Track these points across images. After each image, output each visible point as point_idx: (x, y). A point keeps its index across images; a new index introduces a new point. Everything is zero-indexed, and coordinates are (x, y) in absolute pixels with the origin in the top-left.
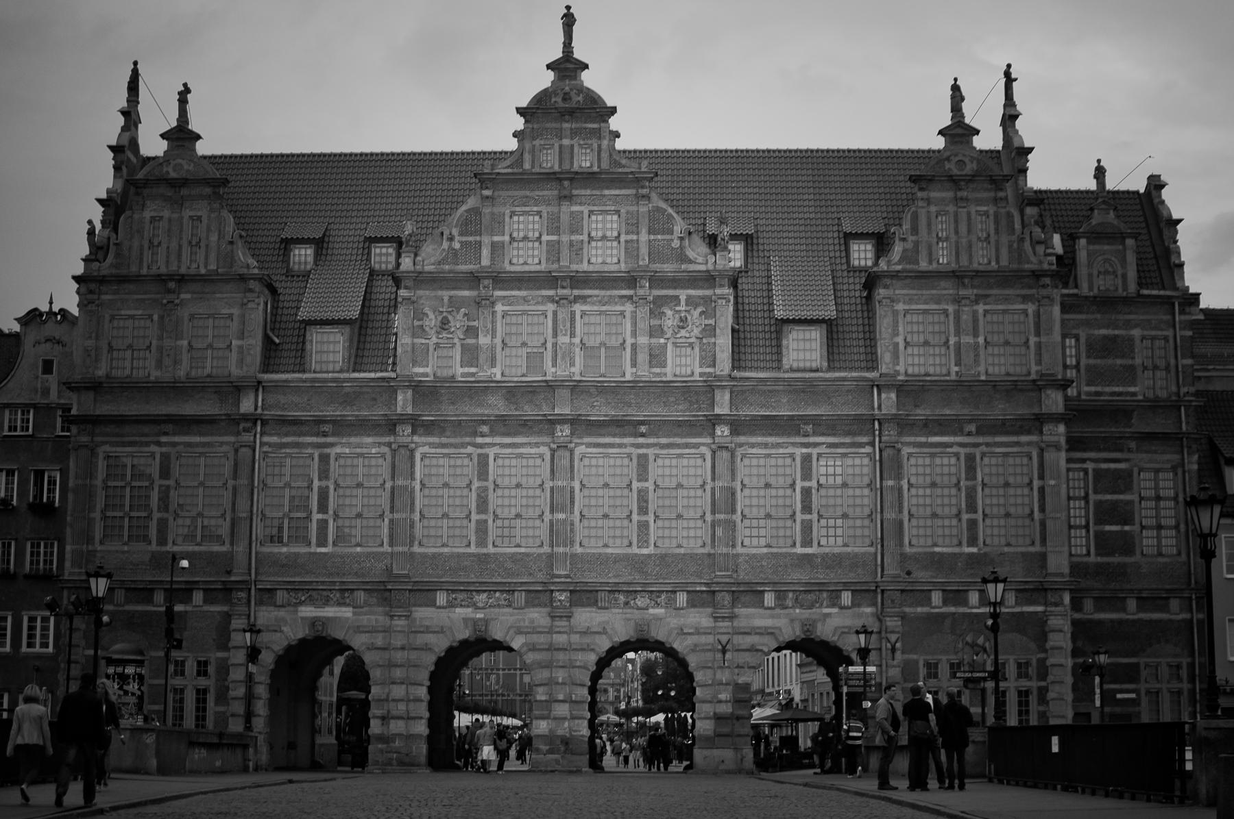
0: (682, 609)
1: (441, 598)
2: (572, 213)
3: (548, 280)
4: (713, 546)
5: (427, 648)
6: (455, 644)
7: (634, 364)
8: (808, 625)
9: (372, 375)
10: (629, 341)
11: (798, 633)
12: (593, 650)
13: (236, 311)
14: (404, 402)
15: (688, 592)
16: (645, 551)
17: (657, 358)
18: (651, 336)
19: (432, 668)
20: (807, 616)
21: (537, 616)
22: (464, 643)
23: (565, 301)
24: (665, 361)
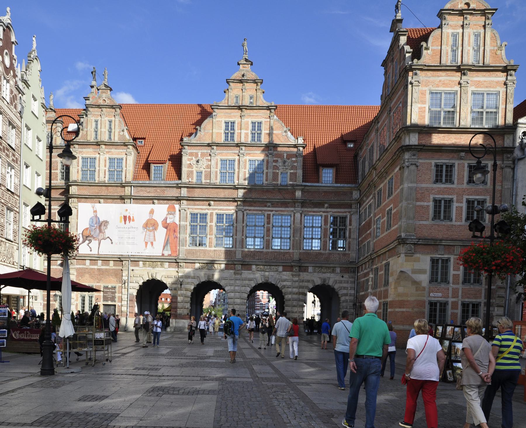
0: (281, 272)
4: (293, 249)
7: (266, 180)
8: (324, 280)
9: (173, 182)
10: (265, 171)
13: (124, 156)
14: (184, 192)
16: (268, 250)
19: (192, 291)
20: (323, 276)
22: (203, 283)
23: (242, 155)
24: (278, 179)
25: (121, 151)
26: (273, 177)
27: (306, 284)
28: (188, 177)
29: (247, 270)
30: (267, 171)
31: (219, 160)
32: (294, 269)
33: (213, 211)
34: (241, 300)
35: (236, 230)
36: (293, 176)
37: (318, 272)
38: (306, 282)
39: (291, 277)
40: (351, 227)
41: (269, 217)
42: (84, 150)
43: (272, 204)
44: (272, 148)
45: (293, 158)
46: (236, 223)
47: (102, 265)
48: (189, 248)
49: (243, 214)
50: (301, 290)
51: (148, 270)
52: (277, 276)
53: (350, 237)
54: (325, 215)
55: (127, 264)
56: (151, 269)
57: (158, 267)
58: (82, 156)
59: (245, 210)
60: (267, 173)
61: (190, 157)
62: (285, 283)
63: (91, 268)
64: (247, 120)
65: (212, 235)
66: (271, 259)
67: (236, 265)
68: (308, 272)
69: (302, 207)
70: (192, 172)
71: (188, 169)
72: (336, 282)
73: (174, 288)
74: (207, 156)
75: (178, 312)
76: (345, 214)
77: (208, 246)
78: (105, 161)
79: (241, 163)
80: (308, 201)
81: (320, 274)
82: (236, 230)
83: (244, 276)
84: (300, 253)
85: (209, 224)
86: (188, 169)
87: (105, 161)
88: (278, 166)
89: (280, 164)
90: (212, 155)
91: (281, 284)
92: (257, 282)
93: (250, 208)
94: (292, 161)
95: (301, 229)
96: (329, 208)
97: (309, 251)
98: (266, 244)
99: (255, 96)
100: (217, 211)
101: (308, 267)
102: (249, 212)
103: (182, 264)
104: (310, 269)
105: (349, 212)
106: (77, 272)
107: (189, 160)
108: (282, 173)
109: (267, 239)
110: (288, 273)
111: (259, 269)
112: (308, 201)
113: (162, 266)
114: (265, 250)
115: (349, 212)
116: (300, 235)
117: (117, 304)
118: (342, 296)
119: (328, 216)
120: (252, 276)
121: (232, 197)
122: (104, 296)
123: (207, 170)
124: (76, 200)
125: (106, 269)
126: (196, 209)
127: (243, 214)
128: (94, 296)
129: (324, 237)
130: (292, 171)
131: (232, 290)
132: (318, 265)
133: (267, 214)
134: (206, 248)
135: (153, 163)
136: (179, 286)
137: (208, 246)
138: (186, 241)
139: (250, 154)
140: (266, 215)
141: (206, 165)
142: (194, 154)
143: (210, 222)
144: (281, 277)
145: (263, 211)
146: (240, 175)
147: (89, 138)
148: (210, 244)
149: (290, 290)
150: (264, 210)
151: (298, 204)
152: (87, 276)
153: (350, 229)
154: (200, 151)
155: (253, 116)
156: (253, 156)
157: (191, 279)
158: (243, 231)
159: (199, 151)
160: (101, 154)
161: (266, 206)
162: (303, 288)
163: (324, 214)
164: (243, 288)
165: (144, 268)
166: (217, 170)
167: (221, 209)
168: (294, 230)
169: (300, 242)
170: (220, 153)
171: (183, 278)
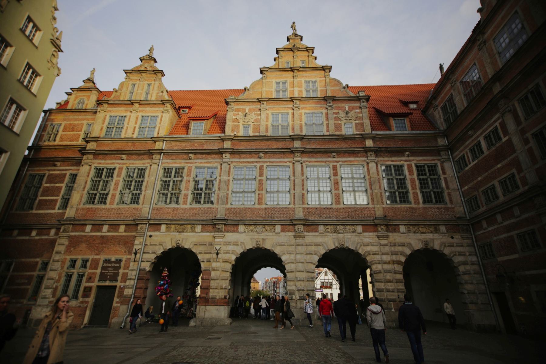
0: (361, 233)
1: (241, 228)
3: (292, 99)
4: (373, 204)
5: (233, 252)
6: (245, 251)
8: (426, 243)
11: (421, 246)
12: (315, 254)
14: (227, 145)
15: (362, 225)
16: (339, 206)
17: (338, 127)
18: (335, 121)
19: (234, 263)
21: (287, 237)
23: (297, 109)
25: (158, 109)
26: (335, 127)
27: (400, 249)
29: (312, 232)
30: (327, 122)
31: (270, 114)
32: (380, 229)
33: (263, 164)
35: (294, 184)
36: (360, 126)
37: (414, 232)
38: (399, 246)
39: (377, 239)
40: (445, 176)
41: (335, 168)
42: (114, 109)
44: (331, 101)
46: (294, 176)
47: (108, 231)
48: (231, 206)
49: (302, 166)
50: (394, 258)
51: (172, 235)
52: (357, 239)
53: (448, 188)
54: (408, 165)
55: (144, 227)
56: (177, 234)
57: (186, 232)
58: (110, 114)
59: (304, 162)
60: (328, 125)
63: (91, 236)
64: (300, 80)
65: (262, 190)
66: (345, 217)
67: (297, 226)
68: (399, 232)
69: (376, 156)
70: (238, 126)
71: (233, 124)
72: (443, 244)
73: (207, 259)
74: (256, 111)
75: (211, 294)
76: (433, 162)
77: (256, 204)
78: (137, 118)
79: (296, 116)
80: (383, 149)
81: (418, 234)
82: (294, 184)
84: (384, 209)
86: (233, 124)
87: (137, 118)
90: (262, 110)
91: (363, 250)
92: (327, 247)
93: (310, 159)
94: (356, 112)
95: (379, 180)
96: (411, 156)
97: (396, 206)
99: (308, 61)
101: (399, 225)
103: (220, 227)
104: (402, 229)
105: (439, 160)
106: (70, 242)
107: (234, 115)
108: (345, 123)
109: (335, 193)
110: (371, 234)
111: (329, 230)
112: (383, 149)
113: (193, 230)
114: (334, 206)
116: (380, 187)
117: (119, 284)
118: (459, 266)
119: (411, 165)
121: (289, 148)
122: (101, 273)
123: (256, 123)
124: (91, 156)
125: (114, 236)
126: (241, 162)
127: (302, 166)
128: (86, 274)
130: (357, 122)
131: (292, 259)
133: (333, 165)
134: (254, 207)
135: (193, 120)
136: (215, 255)
138: (227, 198)
139: (305, 108)
140: (331, 167)
141: (254, 119)
143: (260, 176)
144: (362, 239)
145: (327, 163)
146: (296, 127)
147: (121, 99)
148: (260, 201)
149: (378, 257)
150: (328, 161)
151: (371, 153)
152: (84, 245)
154: (248, 107)
155: (306, 76)
157: (232, 246)
159: (247, 108)
160: (133, 112)
161: (330, 157)
162: (398, 254)
163: (406, 163)
164: (309, 256)
165: (166, 233)
166: (267, 123)
167: (273, 162)
168: (370, 182)
169: (381, 196)
170: (271, 108)
171: (220, 245)
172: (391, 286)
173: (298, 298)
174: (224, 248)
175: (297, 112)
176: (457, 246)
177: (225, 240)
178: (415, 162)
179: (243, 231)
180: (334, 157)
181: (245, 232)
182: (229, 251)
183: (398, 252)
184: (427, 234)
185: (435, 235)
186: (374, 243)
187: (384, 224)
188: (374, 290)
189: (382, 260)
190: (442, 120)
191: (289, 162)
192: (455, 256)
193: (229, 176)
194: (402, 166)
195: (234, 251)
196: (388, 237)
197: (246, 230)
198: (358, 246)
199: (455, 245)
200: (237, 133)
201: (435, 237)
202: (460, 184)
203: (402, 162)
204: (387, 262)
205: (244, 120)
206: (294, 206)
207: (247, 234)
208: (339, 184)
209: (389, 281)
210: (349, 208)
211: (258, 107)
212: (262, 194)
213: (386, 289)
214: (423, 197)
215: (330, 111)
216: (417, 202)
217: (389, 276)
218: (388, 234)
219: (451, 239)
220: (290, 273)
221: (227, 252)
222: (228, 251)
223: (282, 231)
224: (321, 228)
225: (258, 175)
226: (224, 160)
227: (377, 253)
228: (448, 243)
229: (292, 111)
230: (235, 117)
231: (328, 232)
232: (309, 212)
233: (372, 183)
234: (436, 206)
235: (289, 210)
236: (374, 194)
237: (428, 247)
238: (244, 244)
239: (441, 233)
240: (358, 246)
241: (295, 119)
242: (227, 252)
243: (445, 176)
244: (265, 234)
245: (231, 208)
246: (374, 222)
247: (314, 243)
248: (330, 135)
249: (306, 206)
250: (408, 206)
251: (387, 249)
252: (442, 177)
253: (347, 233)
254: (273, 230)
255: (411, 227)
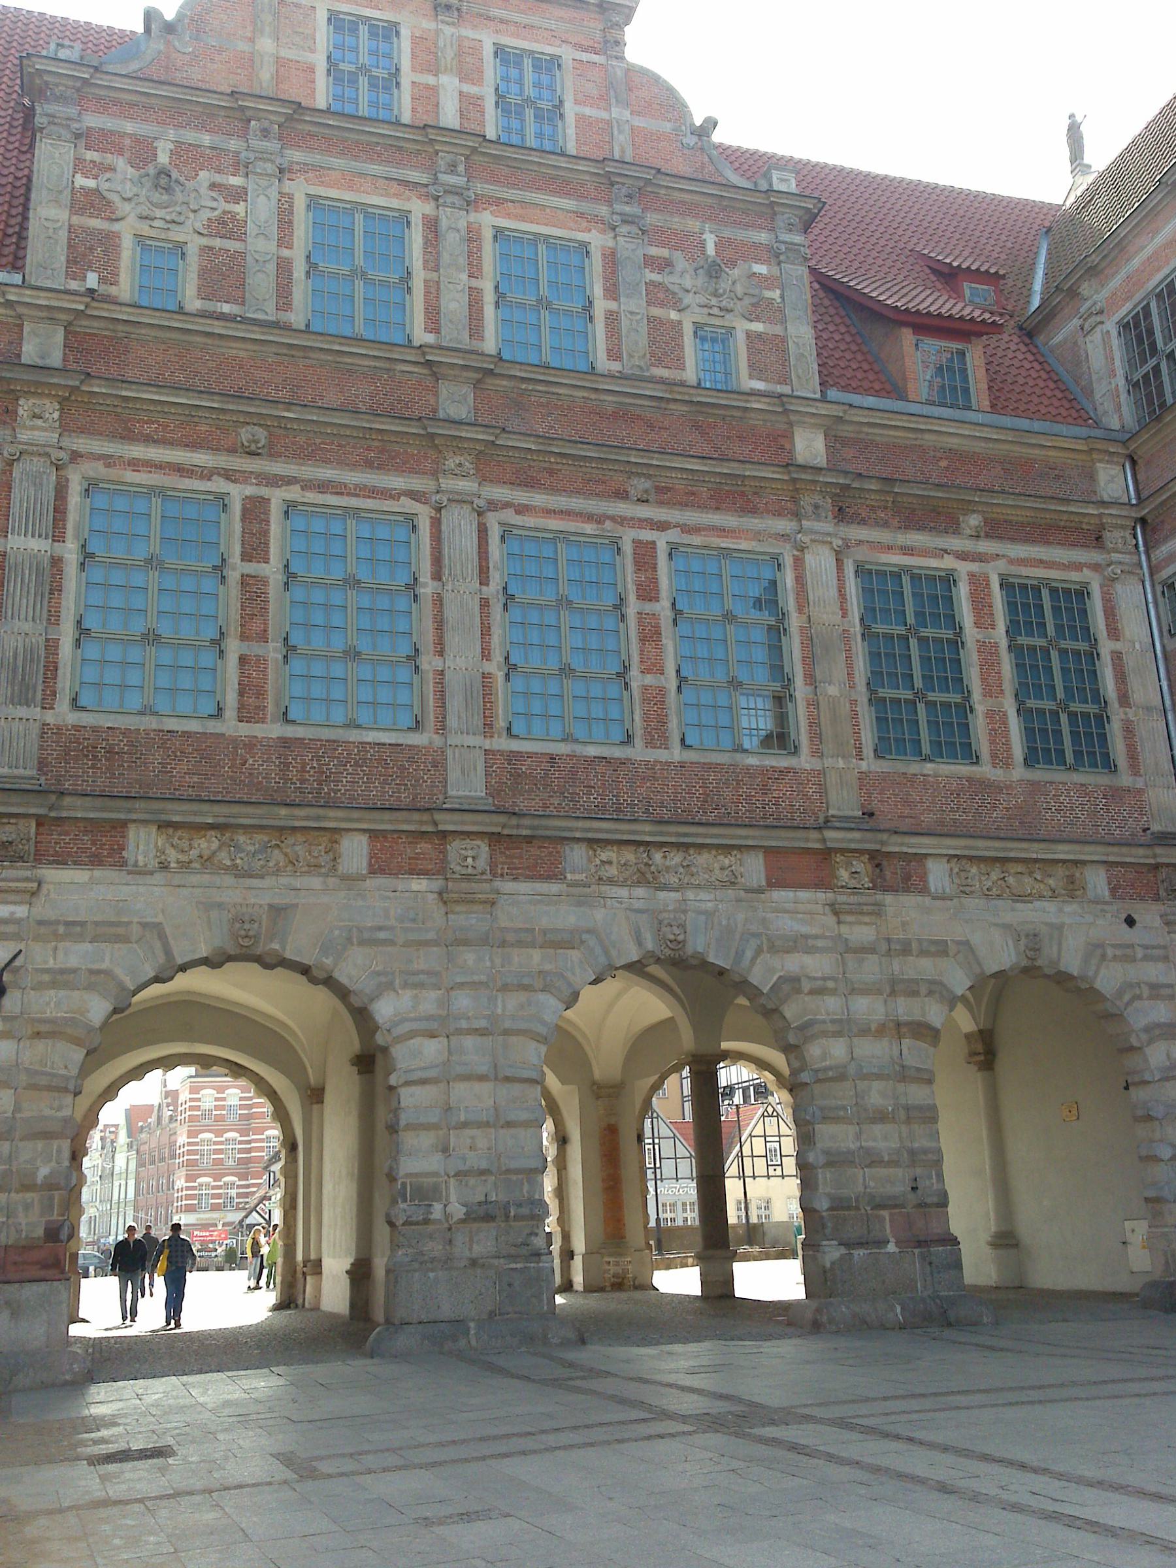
2: (461, 39)
4: (817, 753)
7: (614, 354)
8: (1033, 941)
10: (601, 306)
15: (768, 851)
16: (662, 755)
27: (925, 967)
28: (71, 262)
30: (613, 305)
31: (300, 203)
32: (844, 874)
33: (265, 491)
34: (505, 1092)
38: (923, 953)
39: (831, 920)
40: (1118, 646)
43: (660, 490)
45: (758, 260)
46: (437, 576)
48: (72, 718)
49: (483, 531)
50: (905, 1008)
52: (741, 917)
54: (971, 575)
59: (493, 506)
60: (612, 318)
61: (91, 155)
62: (793, 963)
65: (263, 637)
67: (455, 848)
68: (924, 890)
70: (110, 241)
72: (1096, 950)
76: (1074, 576)
77: (230, 713)
79: (452, 242)
81: (1000, 903)
82: (440, 624)
83: (508, 916)
84: (863, 776)
85: (238, 568)
88: (676, 289)
89: (688, 282)
92: (606, 952)
93: (521, 496)
95: (846, 636)
97: (914, 768)
98: (646, 718)
100: (294, 493)
102: (518, 520)
104: (938, 875)
105: (1096, 567)
107: (79, 165)
108: (698, 327)
109: (645, 688)
110: (804, 895)
111: (613, 871)
115: (1096, 567)
120: (567, 917)
123: (218, 243)
127: (483, 531)
129: (987, 693)
130: (758, 327)
131: (430, 1018)
132: (984, 847)
133: (637, 543)
134: (214, 727)
137: (230, 713)
138: (52, 669)
139: (499, 202)
140: (628, 548)
141: (205, 215)
142: (127, 142)
143: (246, 557)
144: (764, 921)
145: (608, 524)
149: (831, 1005)
150: (613, 518)
153: (1117, 657)
154: (172, 134)
155: (502, 21)
156: (522, 219)
158: (486, 631)
161: (621, 495)
162: (915, 993)
163: (963, 568)
166: (286, 253)
167: (323, 487)
168: (809, 642)
169: (855, 715)
170: (305, 168)
172: (886, 1138)
173: (457, 1211)
174: (41, 956)
175: (454, 220)
176: (1146, 958)
177: (41, 909)
178: (1001, 565)
179: (153, 864)
180: (641, 501)
181: (164, 866)
182: (74, 971)
183: (916, 981)
184: (1038, 904)
185: (1068, 909)
186: (816, 937)
187: (861, 852)
188: (811, 1158)
189: (849, 1021)
190: (1121, 382)
191: (414, 495)
192: (1137, 1004)
193: (58, 536)
194: (949, 580)
195: (98, 972)
196: (878, 914)
197: (172, 855)
198: (749, 954)
199: (1140, 953)
200: (101, 280)
201: (1067, 921)
202: (1170, 687)
203: (948, 562)
204: (873, 1027)
205: (144, 210)
206: (438, 741)
207: (177, 879)
208: (664, 641)
209: (881, 1117)
210: (709, 767)
211: (234, 144)
212: (260, 661)
213: (868, 1151)
214: (1029, 733)
215: (630, 248)
216: (1002, 758)
217: (877, 1095)
218: (879, 897)
219: (1125, 926)
220: (417, 1090)
221: (61, 979)
222: (62, 971)
223: (377, 867)
224: (577, 855)
225: (237, 549)
226: (24, 436)
227: (830, 984)
228: (1114, 946)
229: (428, 208)
230: (91, 183)
231: (611, 881)
232: (517, 776)
233: (818, 651)
234: (1077, 778)
235: (411, 760)
236: (823, 705)
237: (1039, 963)
238: (162, 937)
239: (1090, 901)
240: (749, 954)
241: (445, 258)
242: (61, 979)
243: (1118, 646)
244: (283, 880)
245: (77, 728)
246: (824, 840)
247: (544, 932)
248: (622, 377)
249: (502, 743)
250: (965, 770)
251: (871, 969)
252: (1106, 647)
253: (698, 886)
254: (324, 859)
255: (974, 870)
